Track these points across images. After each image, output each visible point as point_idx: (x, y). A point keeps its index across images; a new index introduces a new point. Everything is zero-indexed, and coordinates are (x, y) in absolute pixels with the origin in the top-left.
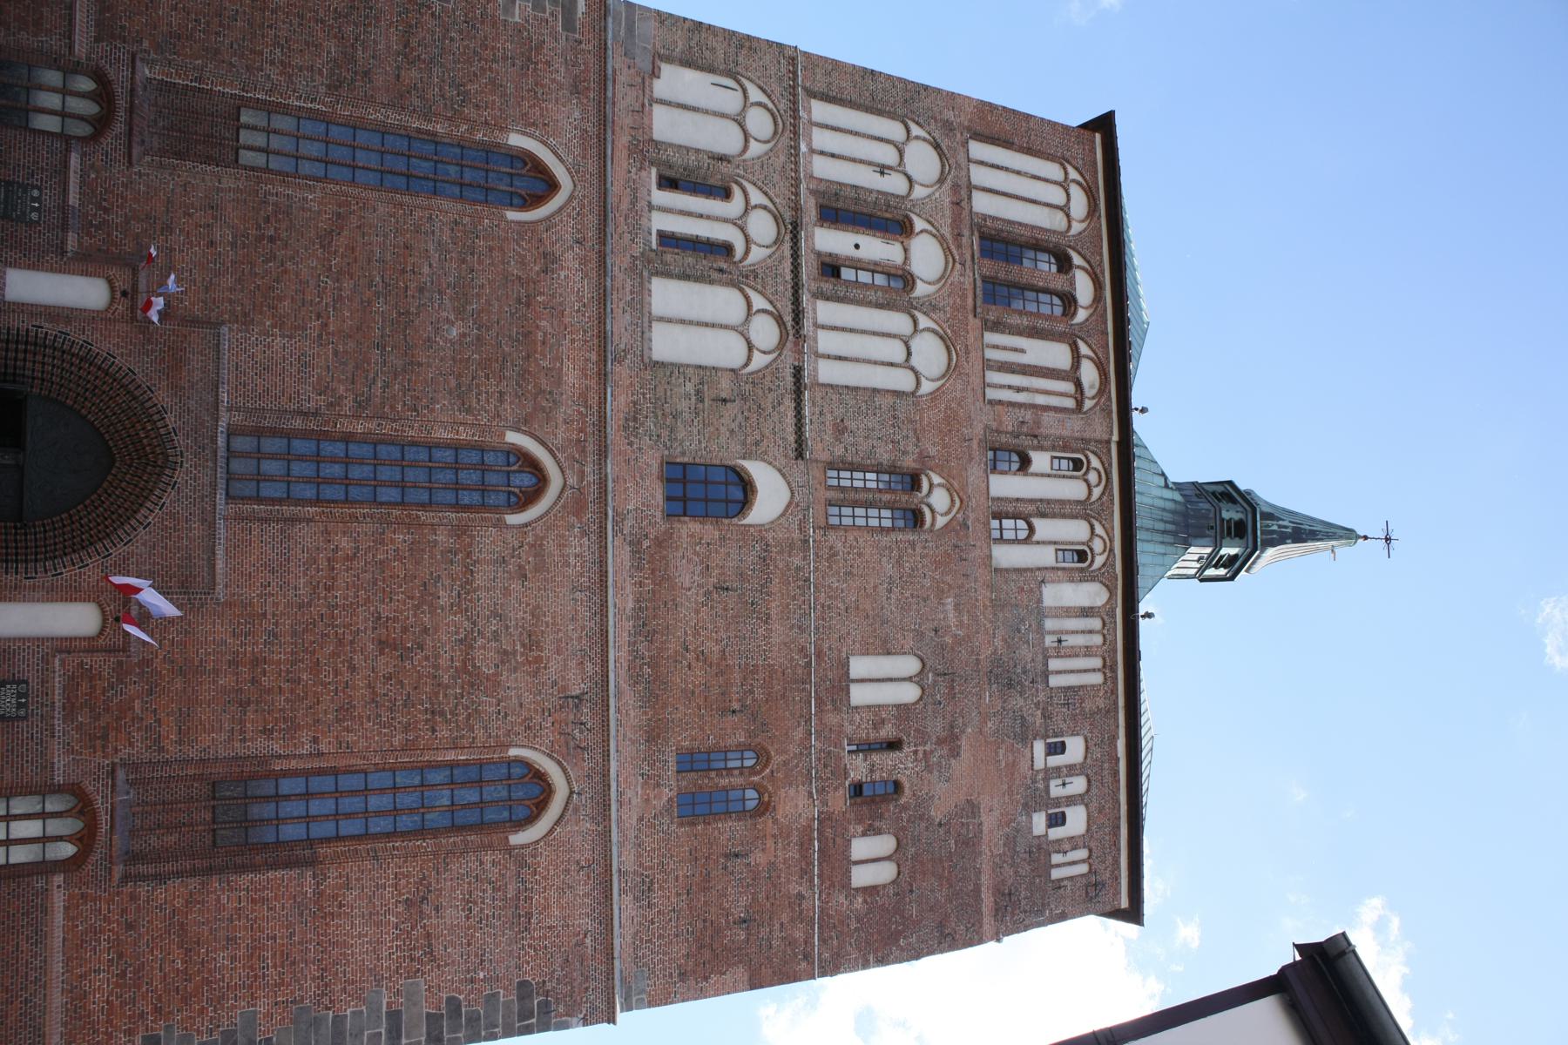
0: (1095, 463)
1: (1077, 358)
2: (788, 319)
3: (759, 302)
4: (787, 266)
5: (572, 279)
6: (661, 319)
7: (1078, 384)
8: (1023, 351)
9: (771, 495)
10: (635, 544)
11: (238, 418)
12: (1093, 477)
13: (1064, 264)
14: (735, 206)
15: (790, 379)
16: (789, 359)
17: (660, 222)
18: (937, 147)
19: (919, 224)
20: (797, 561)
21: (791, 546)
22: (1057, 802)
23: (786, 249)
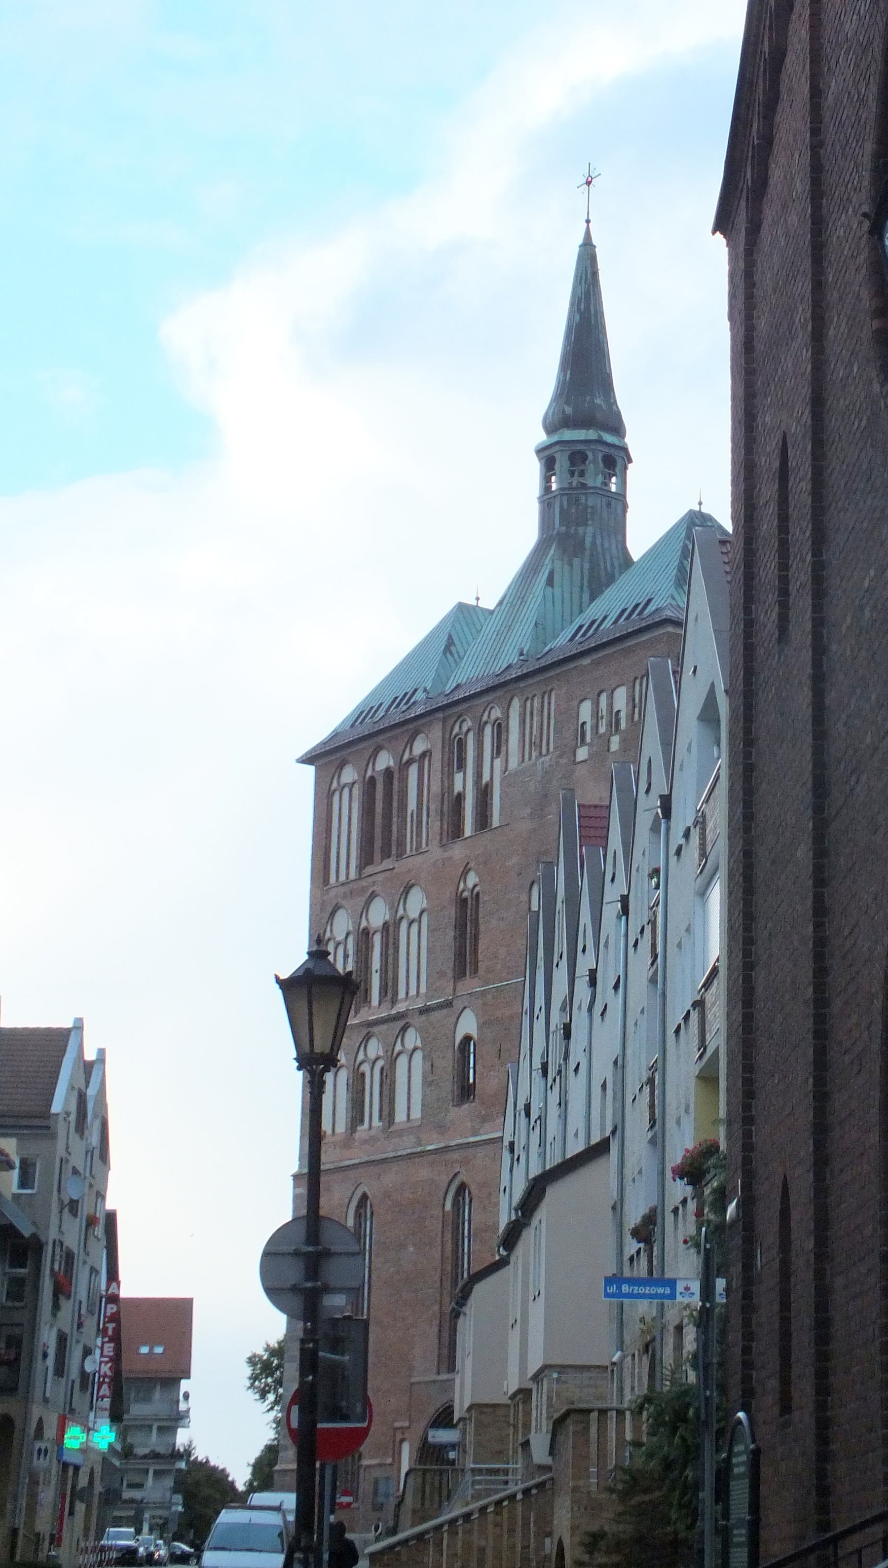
0: (456, 729)
1: (410, 761)
2: (401, 1023)
3: (398, 1047)
4: (383, 1027)
5: (391, 1178)
6: (409, 1115)
7: (424, 755)
8: (412, 814)
9: (468, 1025)
10: (484, 1119)
11: (444, 1368)
12: (465, 729)
13: (372, 780)
14: (366, 1068)
15: (423, 1018)
16: (417, 1020)
17: (376, 1123)
18: (333, 914)
19: (364, 924)
20: (489, 997)
21: (484, 1004)
22: (610, 724)
23: (376, 1030)
